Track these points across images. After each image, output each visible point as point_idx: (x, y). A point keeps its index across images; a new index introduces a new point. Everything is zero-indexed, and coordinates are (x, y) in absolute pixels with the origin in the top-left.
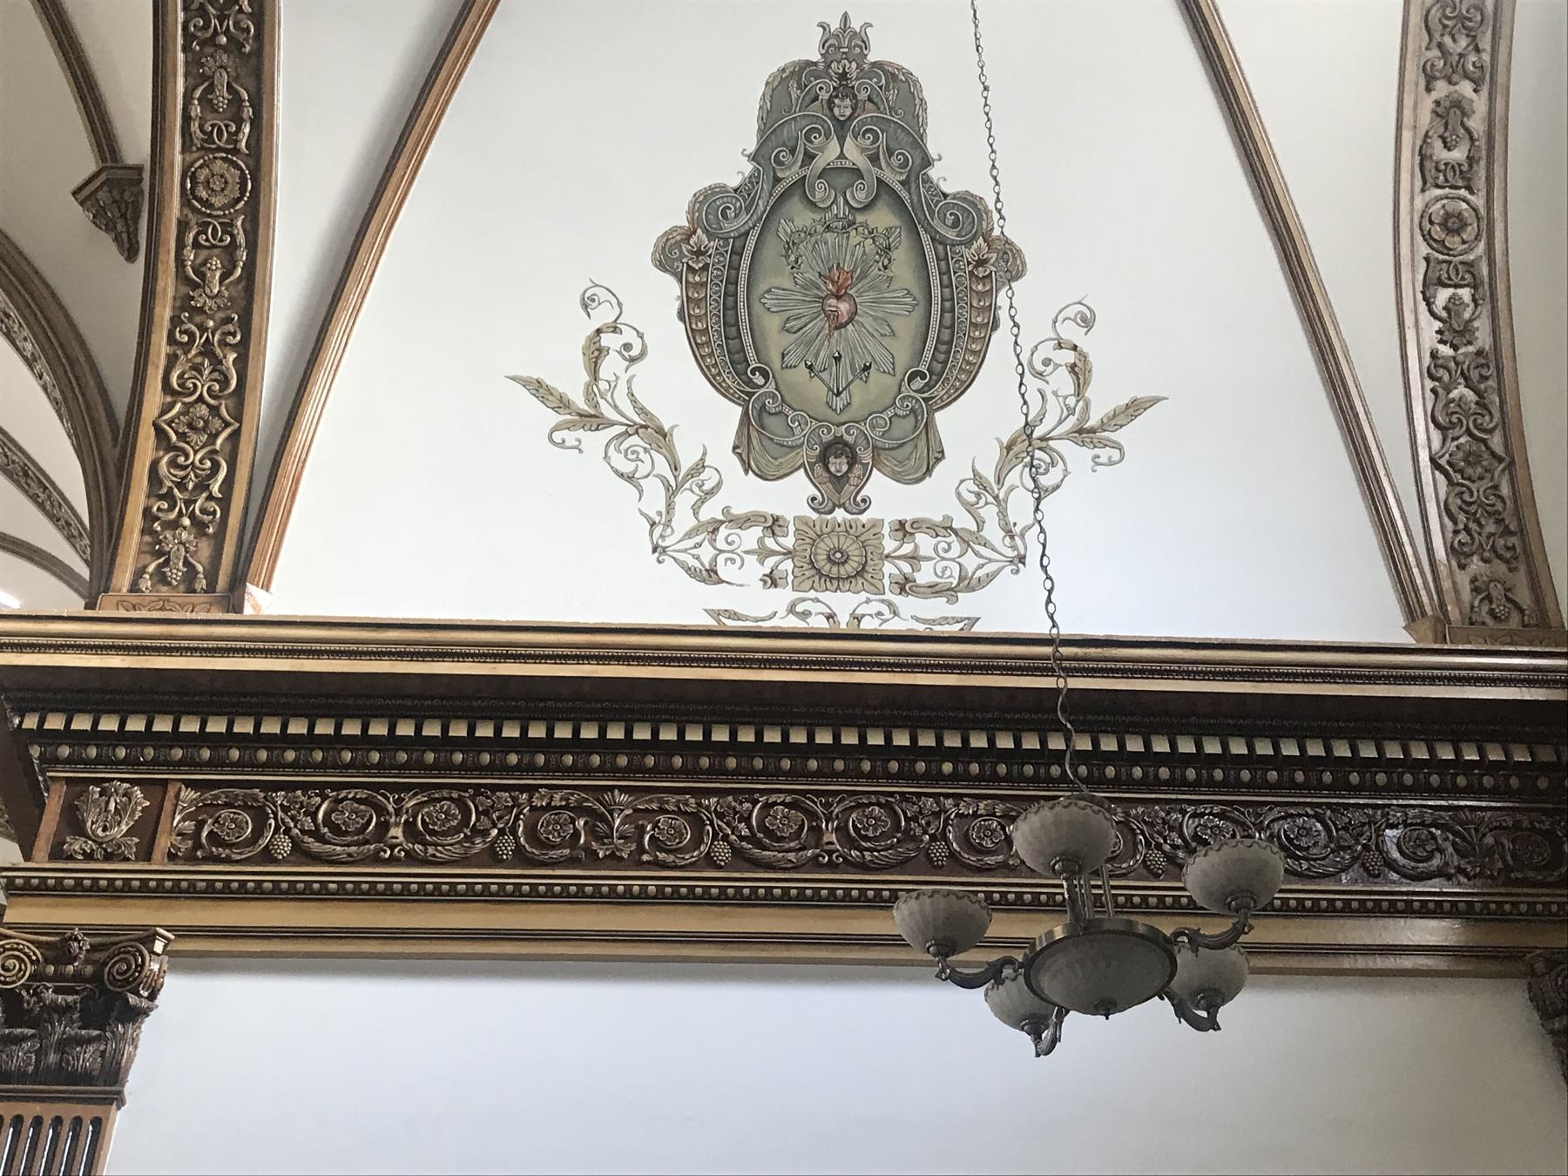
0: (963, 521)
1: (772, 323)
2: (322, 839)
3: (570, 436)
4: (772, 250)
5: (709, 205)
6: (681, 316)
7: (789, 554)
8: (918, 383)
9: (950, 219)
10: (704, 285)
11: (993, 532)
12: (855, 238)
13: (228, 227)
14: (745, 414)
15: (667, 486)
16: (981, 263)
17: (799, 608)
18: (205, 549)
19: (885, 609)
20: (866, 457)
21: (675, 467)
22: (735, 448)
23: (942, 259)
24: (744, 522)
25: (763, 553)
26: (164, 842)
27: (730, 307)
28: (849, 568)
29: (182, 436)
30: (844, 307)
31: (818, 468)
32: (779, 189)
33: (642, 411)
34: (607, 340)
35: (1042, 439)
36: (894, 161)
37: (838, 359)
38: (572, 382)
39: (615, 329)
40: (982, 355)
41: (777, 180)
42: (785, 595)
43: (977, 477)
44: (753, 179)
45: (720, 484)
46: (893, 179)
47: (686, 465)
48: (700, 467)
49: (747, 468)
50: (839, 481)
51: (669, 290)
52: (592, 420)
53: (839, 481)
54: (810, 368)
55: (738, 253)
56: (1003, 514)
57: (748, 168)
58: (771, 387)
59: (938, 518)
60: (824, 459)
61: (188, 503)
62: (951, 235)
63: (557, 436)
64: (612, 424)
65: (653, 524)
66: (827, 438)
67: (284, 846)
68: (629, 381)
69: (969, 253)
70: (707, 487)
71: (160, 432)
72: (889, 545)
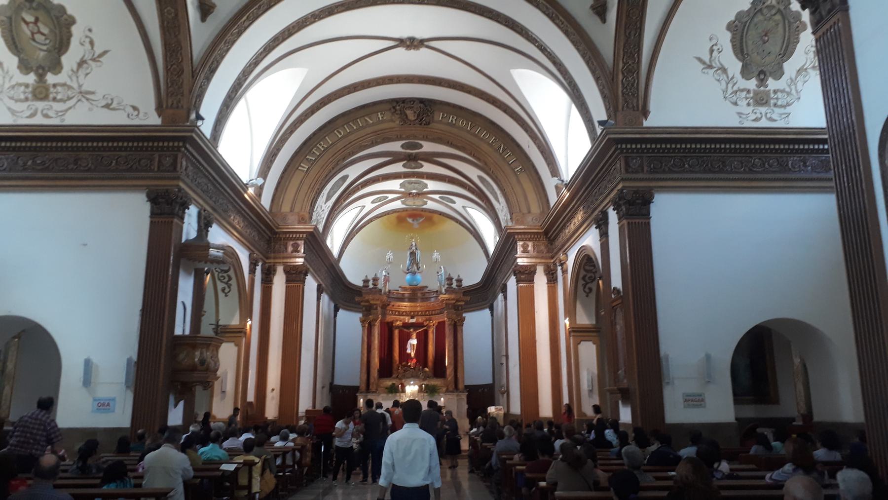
0: (788, 89)
1: (750, 43)
2: (673, 167)
3: (706, 71)
4: (752, 25)
5: (740, 15)
6: (731, 41)
7: (752, 98)
8: (780, 56)
9: (792, 17)
10: (736, 34)
11: (794, 92)
12: (771, 22)
13: (636, 24)
14: (743, 65)
15: (726, 82)
16: (798, 27)
17: (754, 111)
18: (635, 101)
19: (772, 111)
20: (768, 74)
21: (728, 77)
22: (741, 72)
23: (789, 26)
24: (742, 90)
25: (747, 98)
26: (646, 168)
27: (742, 39)
28: (764, 101)
29: (627, 74)
30: (766, 38)
31: (758, 77)
32: (756, 10)
33: (721, 64)
34: (715, 48)
35: (806, 69)
36: (783, 3)
37: (764, 51)
38: (706, 58)
39: (716, 45)
40: (795, 49)
41: (755, 9)
42: (751, 108)
43: (791, 79)
44: (750, 9)
45: (736, 82)
46: (782, 8)
47: (730, 77)
48: (733, 78)
49: (743, 77)
50: (762, 80)
51: (728, 35)
52: (710, 67)
53: (762, 80)
54: (758, 53)
55: (745, 26)
56: (796, 87)
57: (750, 6)
58: (748, 58)
59: (782, 88)
60: (759, 75)
61: (631, 89)
62: (792, 21)
63: (704, 71)
64: (715, 68)
65: (724, 92)
66: (760, 70)
67: (667, 169)
68: (719, 57)
69: (796, 25)
70: (735, 82)
71: (623, 73)
72: (772, 95)
